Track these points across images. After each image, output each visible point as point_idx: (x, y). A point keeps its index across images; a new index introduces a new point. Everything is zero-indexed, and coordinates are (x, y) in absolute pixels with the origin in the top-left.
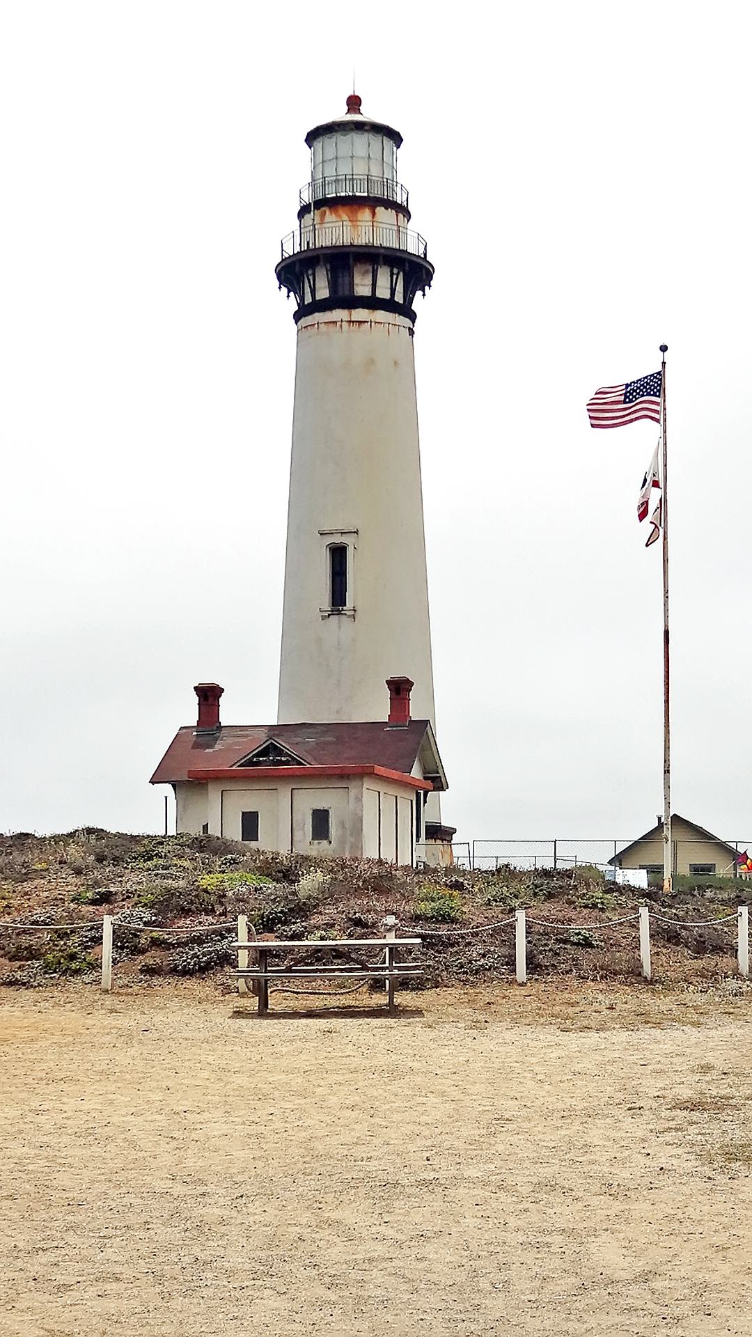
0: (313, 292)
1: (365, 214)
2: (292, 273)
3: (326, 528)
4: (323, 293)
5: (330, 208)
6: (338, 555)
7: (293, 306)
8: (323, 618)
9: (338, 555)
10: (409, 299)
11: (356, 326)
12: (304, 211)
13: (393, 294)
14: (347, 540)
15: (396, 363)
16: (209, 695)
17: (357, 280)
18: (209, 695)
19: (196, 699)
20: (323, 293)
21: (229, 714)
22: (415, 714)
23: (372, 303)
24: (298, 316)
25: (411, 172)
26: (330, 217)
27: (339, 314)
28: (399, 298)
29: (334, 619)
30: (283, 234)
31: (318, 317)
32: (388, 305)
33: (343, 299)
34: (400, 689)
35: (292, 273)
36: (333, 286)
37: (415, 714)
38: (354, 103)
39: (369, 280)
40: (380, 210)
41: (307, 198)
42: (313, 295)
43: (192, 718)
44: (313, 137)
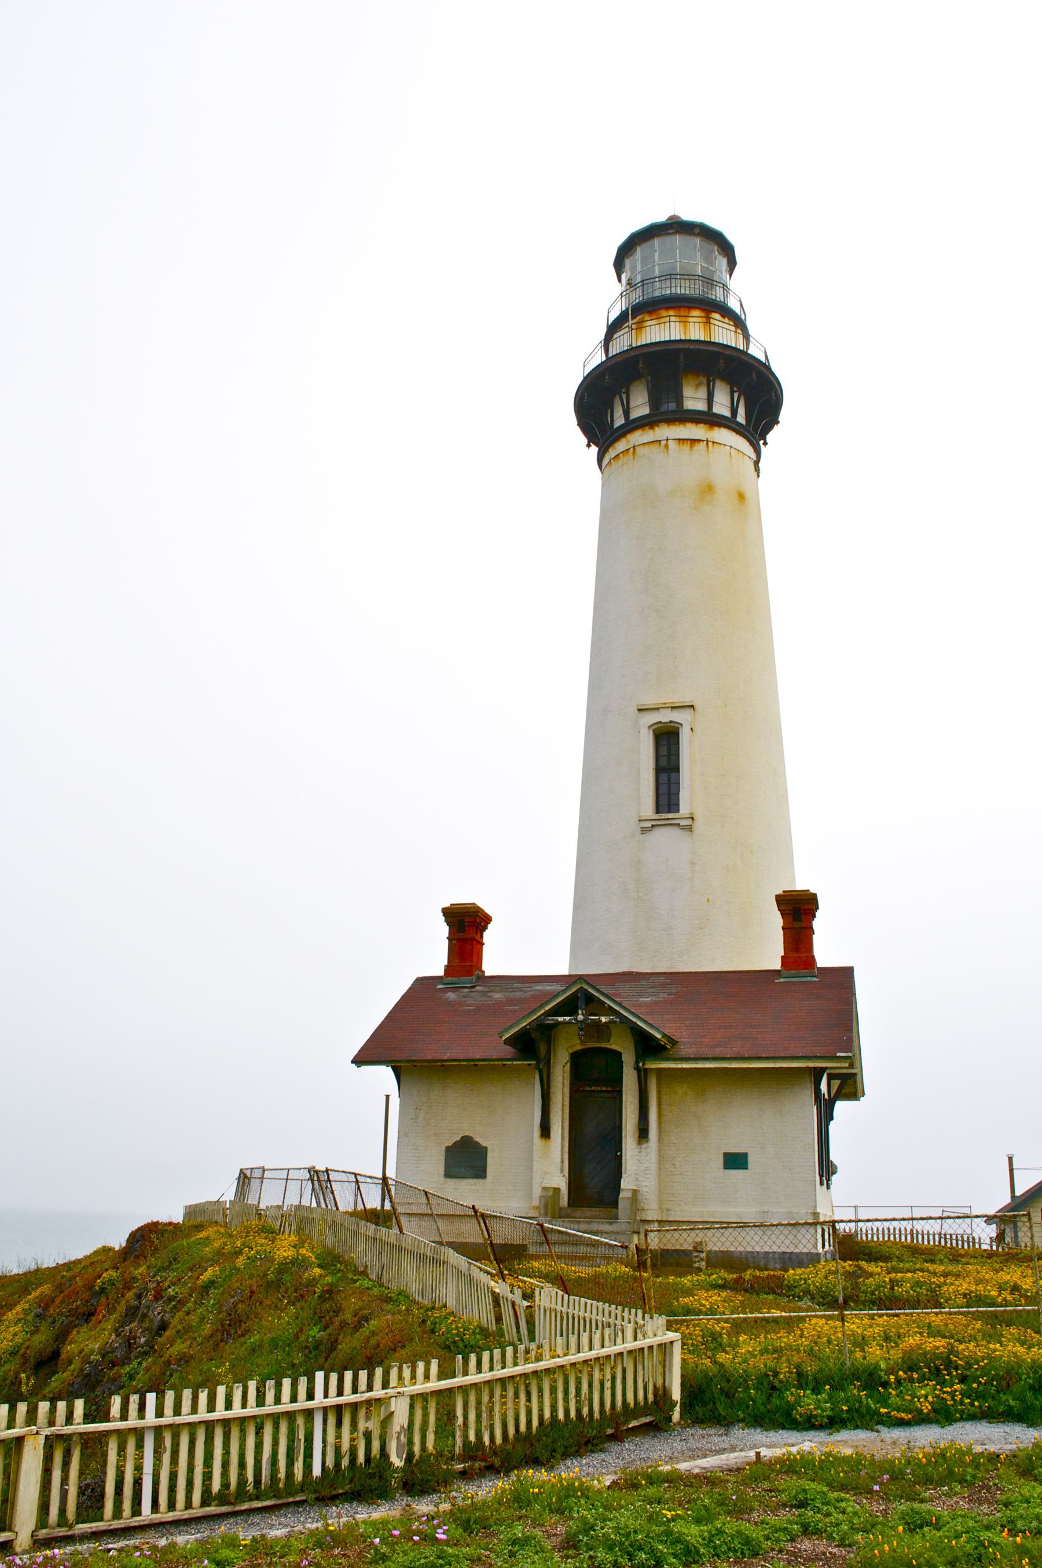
0: (626, 413)
3: (650, 701)
5: (650, 313)
6: (667, 739)
8: (644, 830)
9: (667, 739)
11: (686, 446)
12: (613, 329)
13: (734, 412)
15: (741, 496)
16: (466, 926)
18: (466, 926)
19: (445, 930)
21: (498, 958)
23: (710, 419)
27: (664, 432)
37: (826, 953)
39: (703, 393)
40: (717, 316)
42: (626, 413)
43: (435, 961)
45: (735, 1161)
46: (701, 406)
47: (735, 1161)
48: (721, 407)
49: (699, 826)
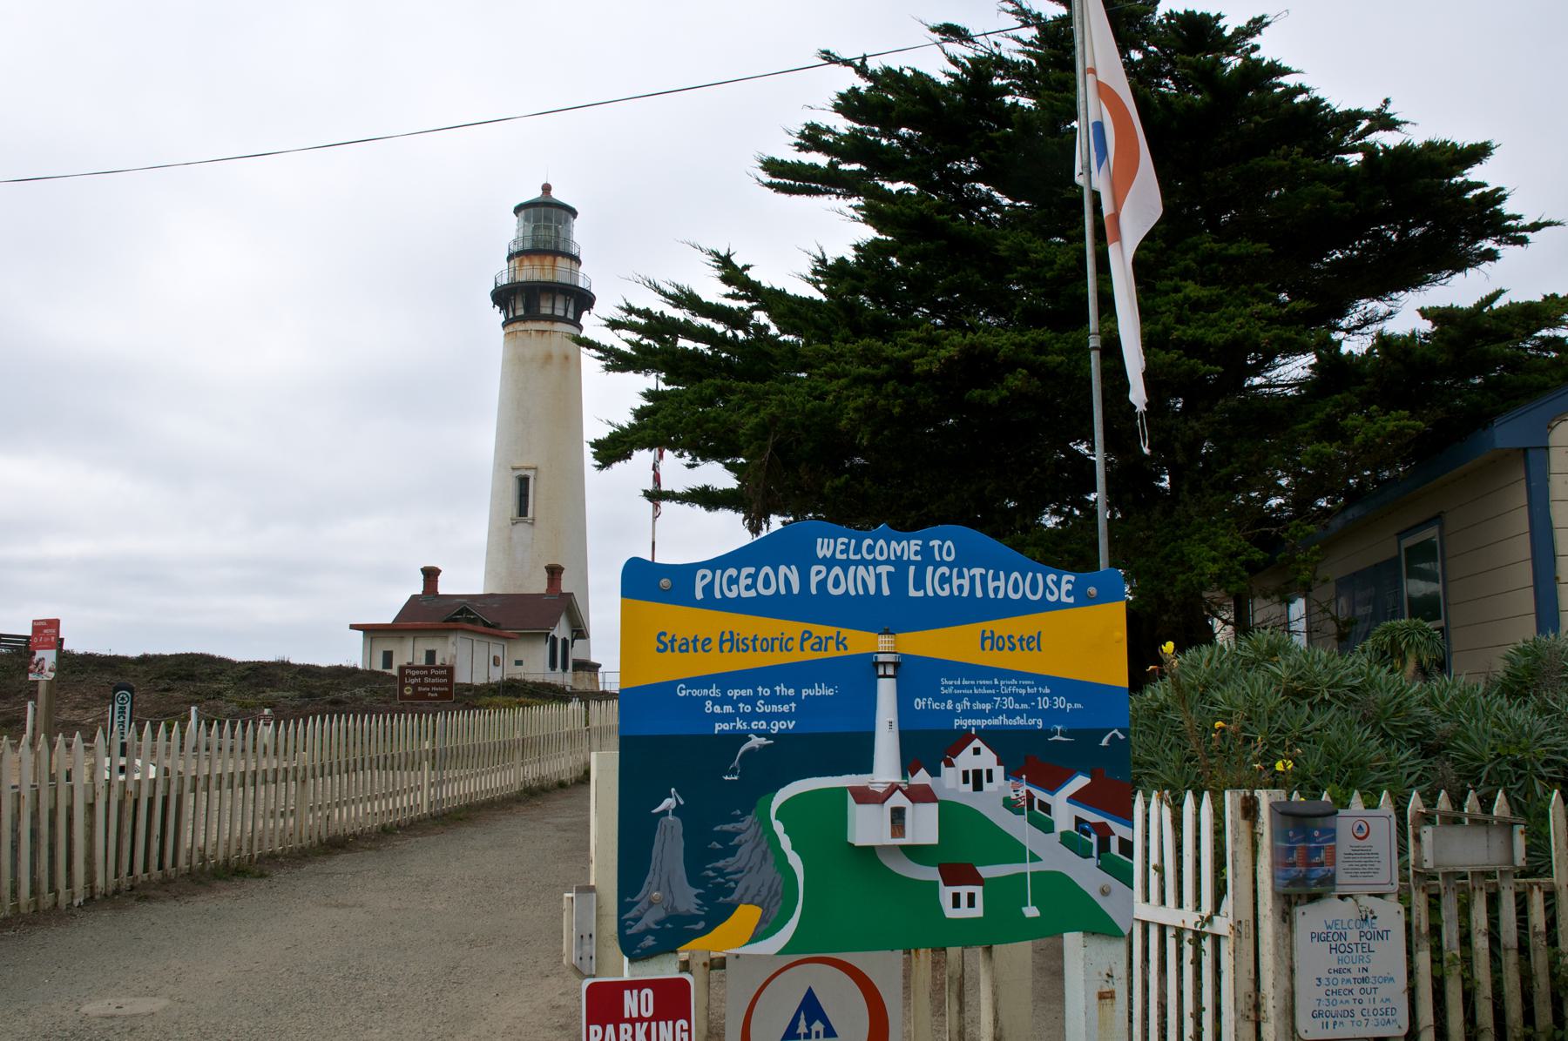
1: (548, 260)
2: (502, 297)
4: (520, 312)
6: (523, 482)
7: (502, 318)
10: (578, 316)
12: (510, 257)
13: (566, 311)
14: (531, 473)
15: (567, 358)
16: (431, 575)
17: (542, 303)
18: (431, 575)
20: (520, 312)
21: (444, 588)
22: (565, 588)
23: (552, 319)
24: (505, 325)
25: (581, 235)
26: (526, 262)
27: (530, 326)
28: (570, 316)
29: (520, 526)
30: (499, 270)
31: (519, 326)
32: (564, 320)
33: (532, 315)
34: (554, 572)
35: (502, 297)
36: (526, 309)
37: (565, 588)
38: (547, 188)
40: (559, 259)
41: (515, 249)
43: (419, 590)
44: (517, 210)
45: (519, 663)
46: (548, 311)
47: (519, 663)
48: (560, 312)
49: (537, 523)
